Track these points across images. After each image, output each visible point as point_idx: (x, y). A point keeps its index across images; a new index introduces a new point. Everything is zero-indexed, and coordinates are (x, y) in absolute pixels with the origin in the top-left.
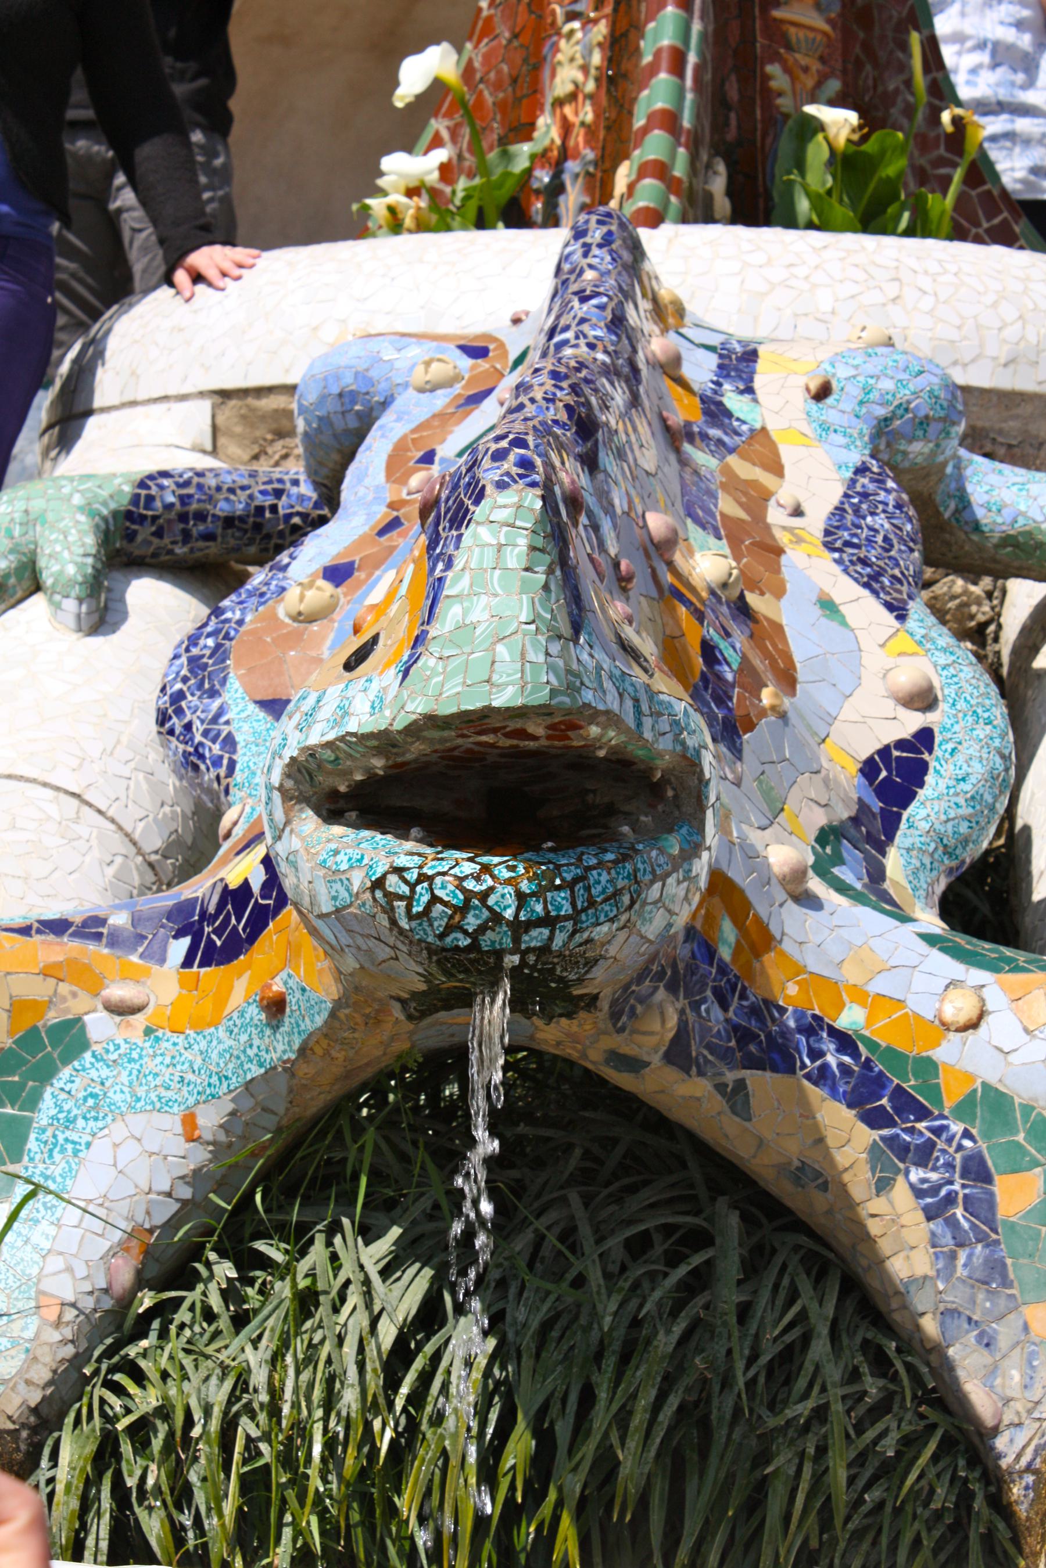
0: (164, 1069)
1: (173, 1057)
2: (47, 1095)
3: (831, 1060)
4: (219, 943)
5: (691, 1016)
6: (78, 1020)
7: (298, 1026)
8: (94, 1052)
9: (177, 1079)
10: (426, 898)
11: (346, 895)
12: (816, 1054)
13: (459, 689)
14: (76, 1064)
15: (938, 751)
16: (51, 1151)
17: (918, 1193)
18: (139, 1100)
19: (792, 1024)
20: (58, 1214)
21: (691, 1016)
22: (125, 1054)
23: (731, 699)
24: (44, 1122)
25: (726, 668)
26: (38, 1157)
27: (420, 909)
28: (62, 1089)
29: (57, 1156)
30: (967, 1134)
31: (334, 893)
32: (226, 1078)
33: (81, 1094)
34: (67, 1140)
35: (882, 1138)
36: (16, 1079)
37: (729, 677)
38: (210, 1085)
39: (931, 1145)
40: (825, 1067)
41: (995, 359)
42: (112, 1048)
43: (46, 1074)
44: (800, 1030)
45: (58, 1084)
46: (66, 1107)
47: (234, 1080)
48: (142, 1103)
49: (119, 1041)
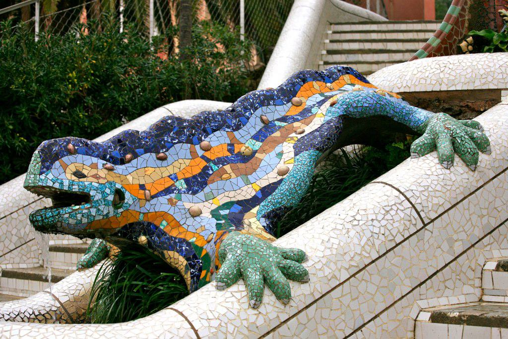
3: (184, 248)
5: (150, 239)
12: (181, 247)
15: (281, 184)
17: (191, 274)
19: (177, 241)
21: (150, 239)
23: (208, 177)
25: (211, 171)
30: (201, 263)
35: (189, 263)
37: (211, 172)
39: (196, 264)
40: (183, 249)
41: (462, 83)
44: (179, 242)
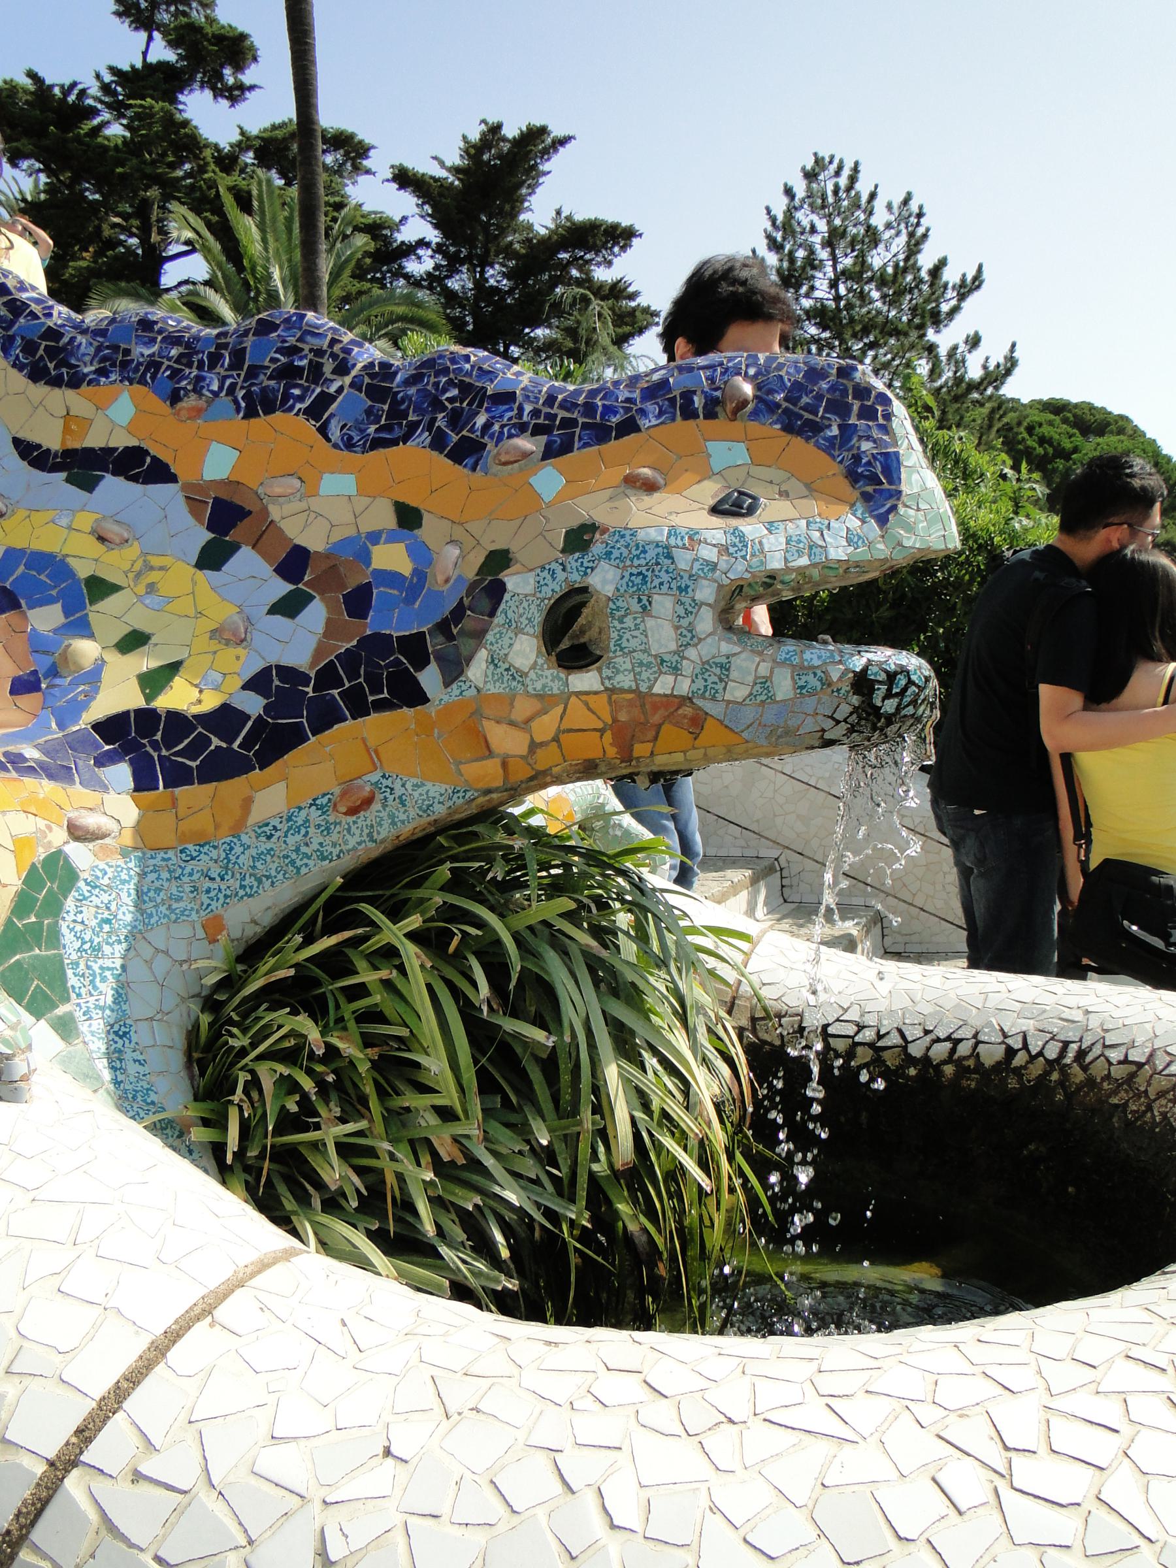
0: (166, 884)
1: (170, 871)
2: (64, 930)
4: (194, 764)
6: (59, 853)
7: (392, 816)
8: (85, 880)
9: (188, 889)
10: (903, 682)
11: (818, 684)
13: (942, 533)
14: (74, 893)
16: (92, 982)
18: (151, 916)
20: (134, 1038)
22: (115, 877)
24: (74, 956)
26: (83, 991)
27: (898, 690)
28: (75, 921)
29: (102, 987)
31: (801, 683)
32: (268, 877)
33: (94, 923)
34: (101, 968)
36: (33, 919)
38: (243, 887)
42: (100, 874)
43: (54, 907)
45: (71, 917)
46: (87, 939)
47: (280, 876)
48: (155, 918)
49: (102, 865)
